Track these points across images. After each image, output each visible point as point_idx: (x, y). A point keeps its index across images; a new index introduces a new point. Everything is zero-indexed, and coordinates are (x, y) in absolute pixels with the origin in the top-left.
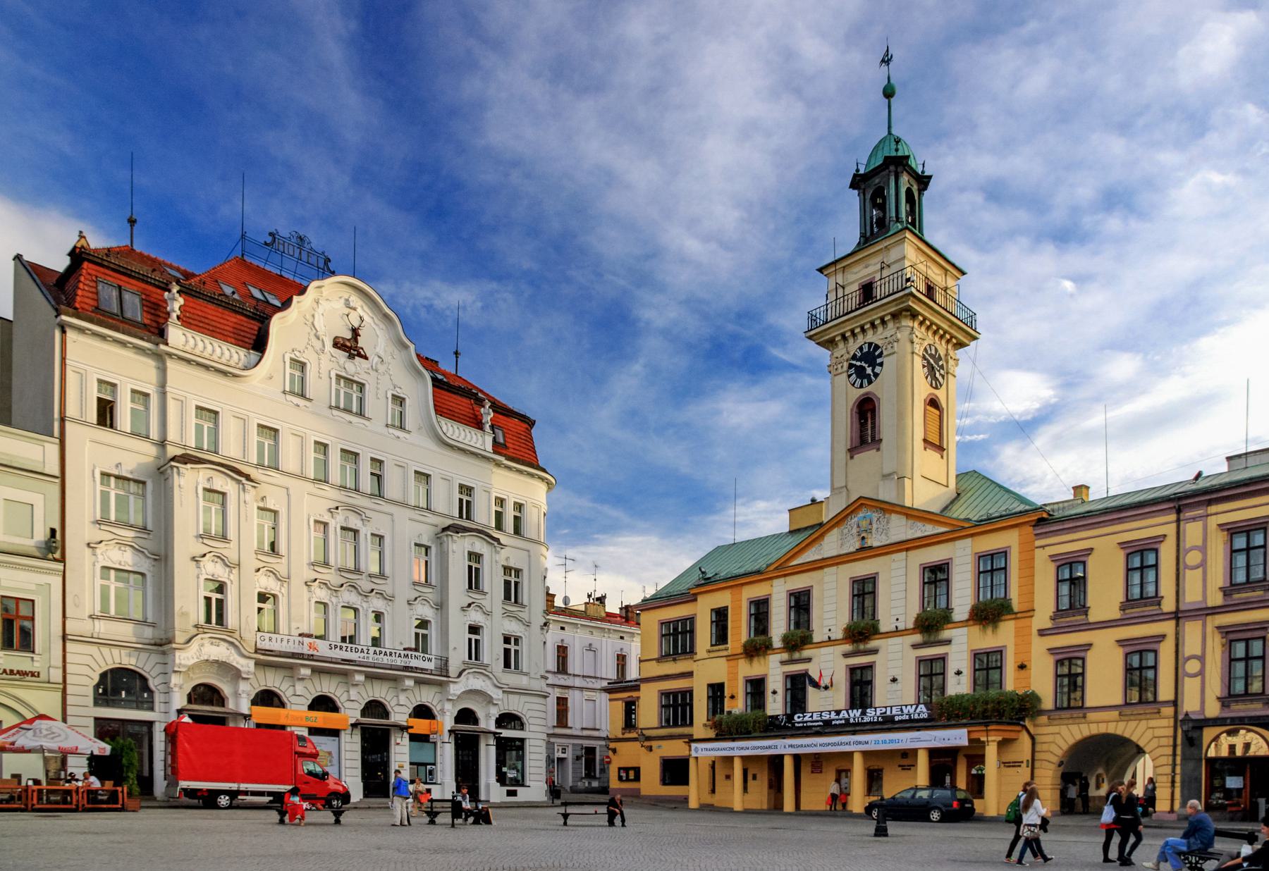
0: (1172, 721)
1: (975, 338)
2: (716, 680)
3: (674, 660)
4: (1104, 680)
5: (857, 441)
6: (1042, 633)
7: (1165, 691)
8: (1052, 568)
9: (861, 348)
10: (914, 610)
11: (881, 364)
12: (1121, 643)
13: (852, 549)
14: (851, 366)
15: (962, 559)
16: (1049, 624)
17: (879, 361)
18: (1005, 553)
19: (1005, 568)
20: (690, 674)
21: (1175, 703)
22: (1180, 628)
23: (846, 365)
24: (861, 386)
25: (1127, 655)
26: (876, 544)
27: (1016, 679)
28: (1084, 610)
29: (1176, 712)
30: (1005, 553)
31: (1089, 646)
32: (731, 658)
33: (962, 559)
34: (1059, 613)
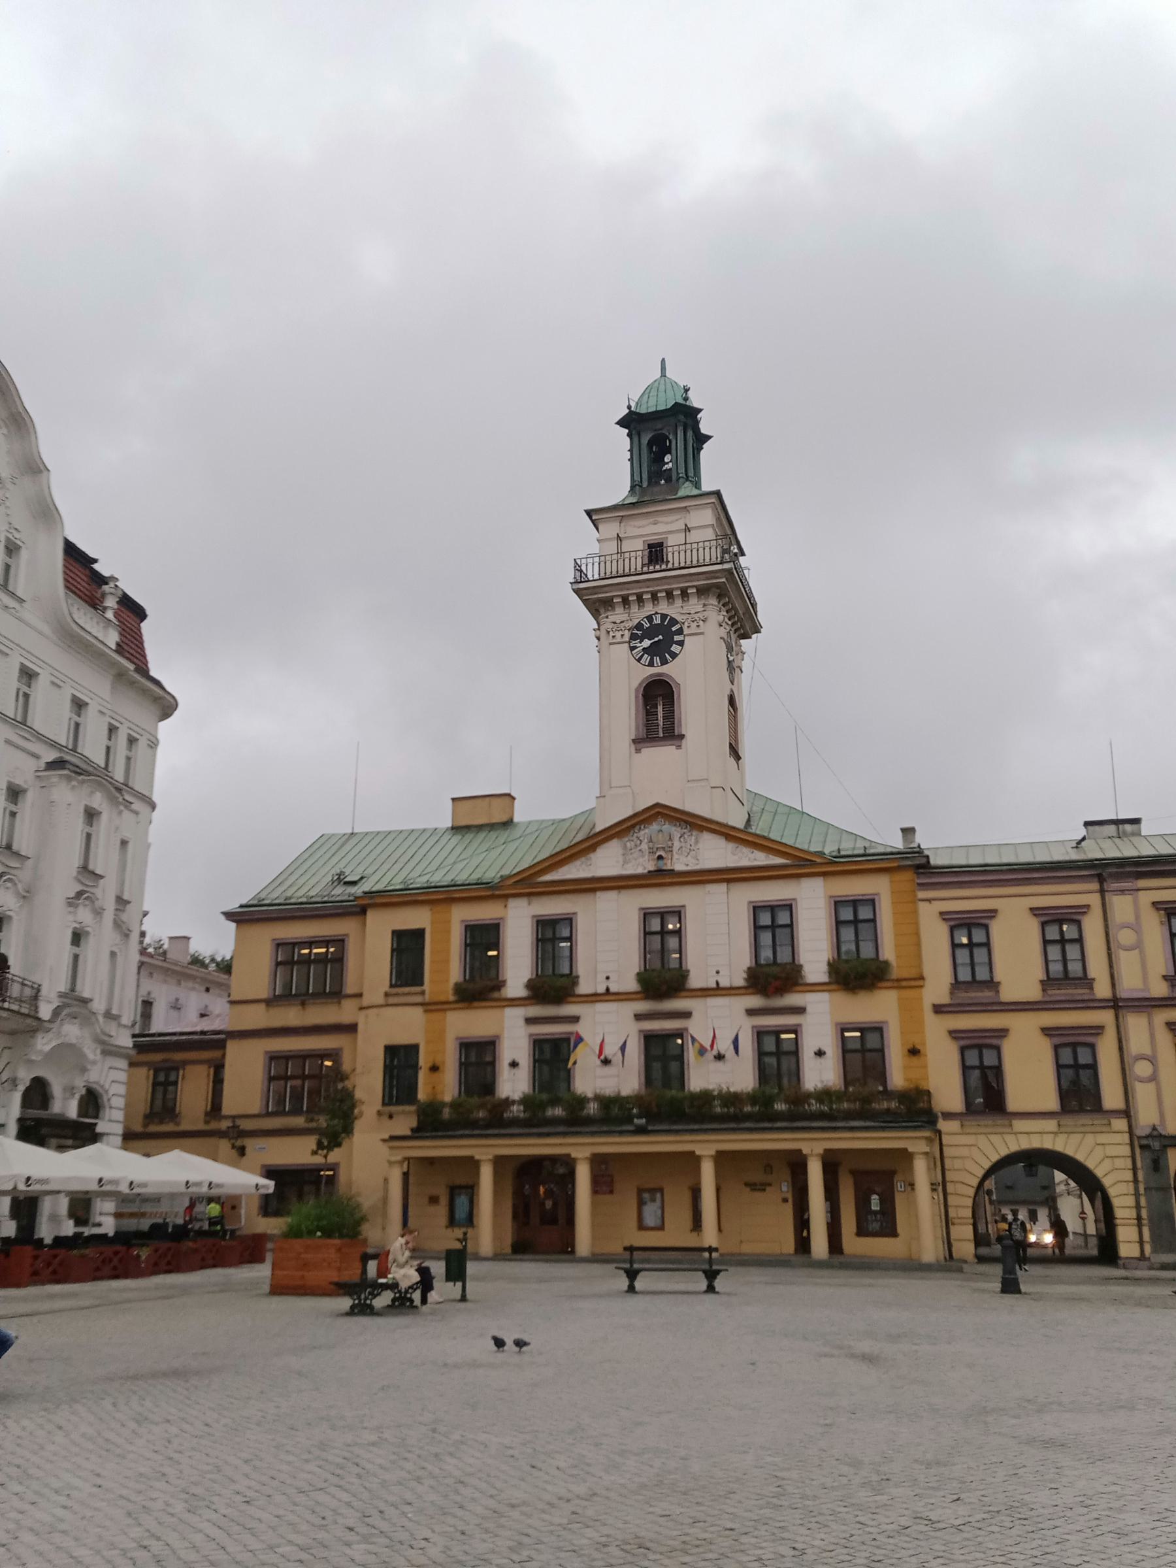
0: (1126, 1136)
2: (402, 1038)
3: (303, 1004)
4: (1030, 1077)
5: (643, 733)
7: (1111, 1097)
8: (943, 930)
9: (650, 618)
10: (745, 960)
11: (681, 643)
12: (1047, 1031)
14: (633, 637)
15: (812, 903)
16: (944, 998)
17: (677, 638)
18: (872, 902)
19: (874, 921)
20: (352, 1028)
21: (1127, 1113)
22: (1121, 1019)
23: (627, 634)
24: (651, 664)
25: (1056, 1048)
27: (906, 1068)
28: (992, 984)
29: (1130, 1127)
30: (872, 902)
31: (1003, 1033)
32: (430, 1007)
33: (812, 903)
34: (957, 985)
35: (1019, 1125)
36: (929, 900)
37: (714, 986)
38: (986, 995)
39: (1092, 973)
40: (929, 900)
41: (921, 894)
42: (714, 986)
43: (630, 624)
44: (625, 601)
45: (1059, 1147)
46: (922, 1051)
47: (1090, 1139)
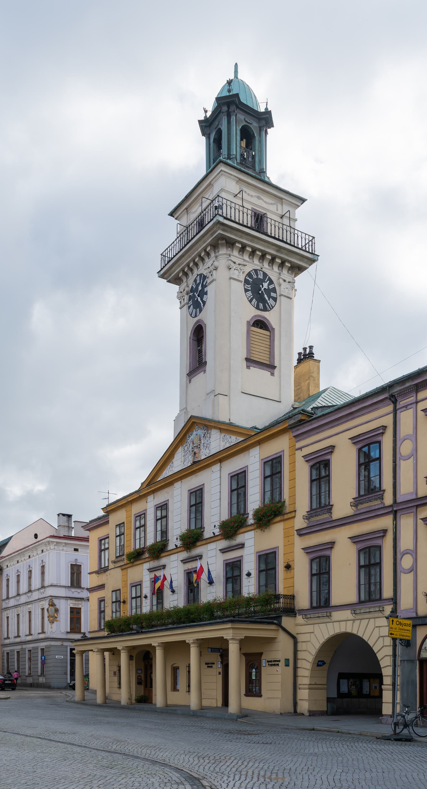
1: (313, 261)
6: (301, 533)
12: (354, 539)
13: (189, 464)
26: (203, 457)
34: (312, 513)
35: (337, 615)
36: (300, 449)
37: (212, 535)
38: (324, 517)
39: (384, 487)
40: (300, 449)
41: (298, 445)
42: (212, 535)
43: (187, 289)
44: (186, 274)
45: (349, 630)
46: (292, 566)
47: (364, 622)
